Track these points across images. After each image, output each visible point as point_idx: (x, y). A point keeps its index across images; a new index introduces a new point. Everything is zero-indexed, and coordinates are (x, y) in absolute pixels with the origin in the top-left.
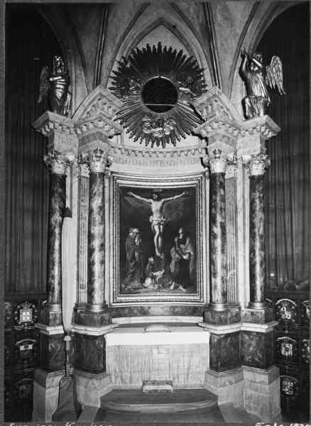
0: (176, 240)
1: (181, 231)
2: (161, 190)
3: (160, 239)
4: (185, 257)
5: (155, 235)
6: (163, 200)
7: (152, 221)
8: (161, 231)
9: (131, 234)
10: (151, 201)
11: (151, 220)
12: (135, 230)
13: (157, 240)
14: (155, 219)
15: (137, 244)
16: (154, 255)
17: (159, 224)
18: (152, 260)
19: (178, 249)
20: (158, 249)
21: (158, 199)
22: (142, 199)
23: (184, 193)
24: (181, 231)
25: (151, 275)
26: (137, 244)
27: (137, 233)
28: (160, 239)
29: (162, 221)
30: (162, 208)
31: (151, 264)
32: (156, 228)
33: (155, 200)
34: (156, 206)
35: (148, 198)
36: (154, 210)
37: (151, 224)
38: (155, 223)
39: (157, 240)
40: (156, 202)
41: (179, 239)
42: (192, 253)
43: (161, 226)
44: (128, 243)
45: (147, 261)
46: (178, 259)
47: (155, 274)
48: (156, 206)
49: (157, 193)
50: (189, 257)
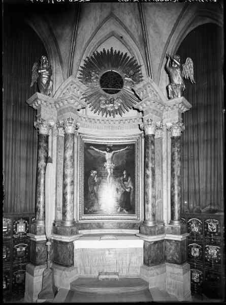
1: (124, 173)
4: (128, 190)
6: (113, 152)
9: (92, 174)
10: (105, 152)
17: (110, 168)
21: (110, 151)
23: (127, 148)
24: (124, 173)
27: (96, 174)
30: (112, 158)
32: (109, 171)
33: (108, 152)
34: (108, 156)
35: (103, 150)
36: (107, 158)
41: (123, 178)
42: (132, 187)
43: (112, 170)
44: (90, 181)
48: (108, 156)
49: (109, 147)
50: (130, 190)
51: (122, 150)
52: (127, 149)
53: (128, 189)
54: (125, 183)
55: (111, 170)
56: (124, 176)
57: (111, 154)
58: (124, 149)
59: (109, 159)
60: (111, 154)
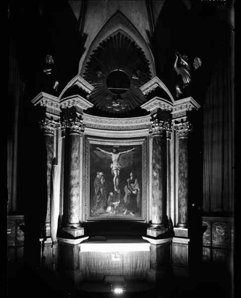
1: (131, 174)
3: (117, 179)
5: (114, 177)
6: (120, 153)
9: (98, 176)
10: (112, 153)
11: (111, 167)
12: (101, 173)
13: (116, 181)
14: (114, 166)
15: (102, 183)
16: (113, 190)
19: (129, 186)
21: (117, 153)
22: (105, 152)
23: (134, 149)
24: (131, 174)
25: (111, 204)
26: (102, 183)
28: (117, 179)
31: (111, 197)
32: (115, 172)
33: (114, 153)
34: (115, 157)
36: (113, 160)
38: (114, 168)
39: (116, 181)
42: (139, 190)
43: (118, 171)
44: (96, 182)
46: (129, 193)
47: (114, 203)
48: (115, 157)
51: (129, 151)
52: (133, 151)
54: (132, 185)
55: (117, 172)
57: (117, 156)
59: (115, 160)
60: (117, 156)
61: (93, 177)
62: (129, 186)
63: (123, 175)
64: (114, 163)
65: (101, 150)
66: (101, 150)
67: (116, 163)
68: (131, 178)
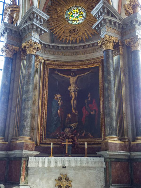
0: (86, 101)
1: (89, 95)
2: (76, 70)
3: (75, 101)
4: (92, 113)
6: (77, 76)
7: (70, 89)
8: (76, 96)
9: (56, 98)
10: (70, 77)
11: (69, 89)
12: (58, 96)
14: (72, 88)
15: (60, 105)
16: (71, 112)
17: (75, 92)
18: (70, 115)
19: (87, 107)
20: (74, 108)
21: (74, 76)
23: (91, 71)
24: (89, 95)
26: (60, 105)
27: (60, 98)
28: (75, 101)
29: (76, 89)
30: (76, 81)
31: (69, 119)
32: (73, 94)
33: (72, 76)
34: (72, 80)
35: (68, 75)
36: (71, 82)
37: (69, 91)
38: (72, 90)
40: (73, 77)
41: (88, 101)
43: (76, 93)
44: (54, 103)
45: (66, 116)
47: (71, 125)
48: (72, 80)
49: (74, 72)
51: (86, 73)
52: (90, 73)
53: (92, 111)
55: (75, 94)
56: (88, 99)
57: (75, 78)
58: (89, 72)
59: (73, 82)
60: (75, 78)
61: (51, 98)
62: (87, 107)
63: (81, 95)
64: (72, 86)
65: (59, 74)
66: (59, 74)
67: (74, 86)
68: (89, 98)
